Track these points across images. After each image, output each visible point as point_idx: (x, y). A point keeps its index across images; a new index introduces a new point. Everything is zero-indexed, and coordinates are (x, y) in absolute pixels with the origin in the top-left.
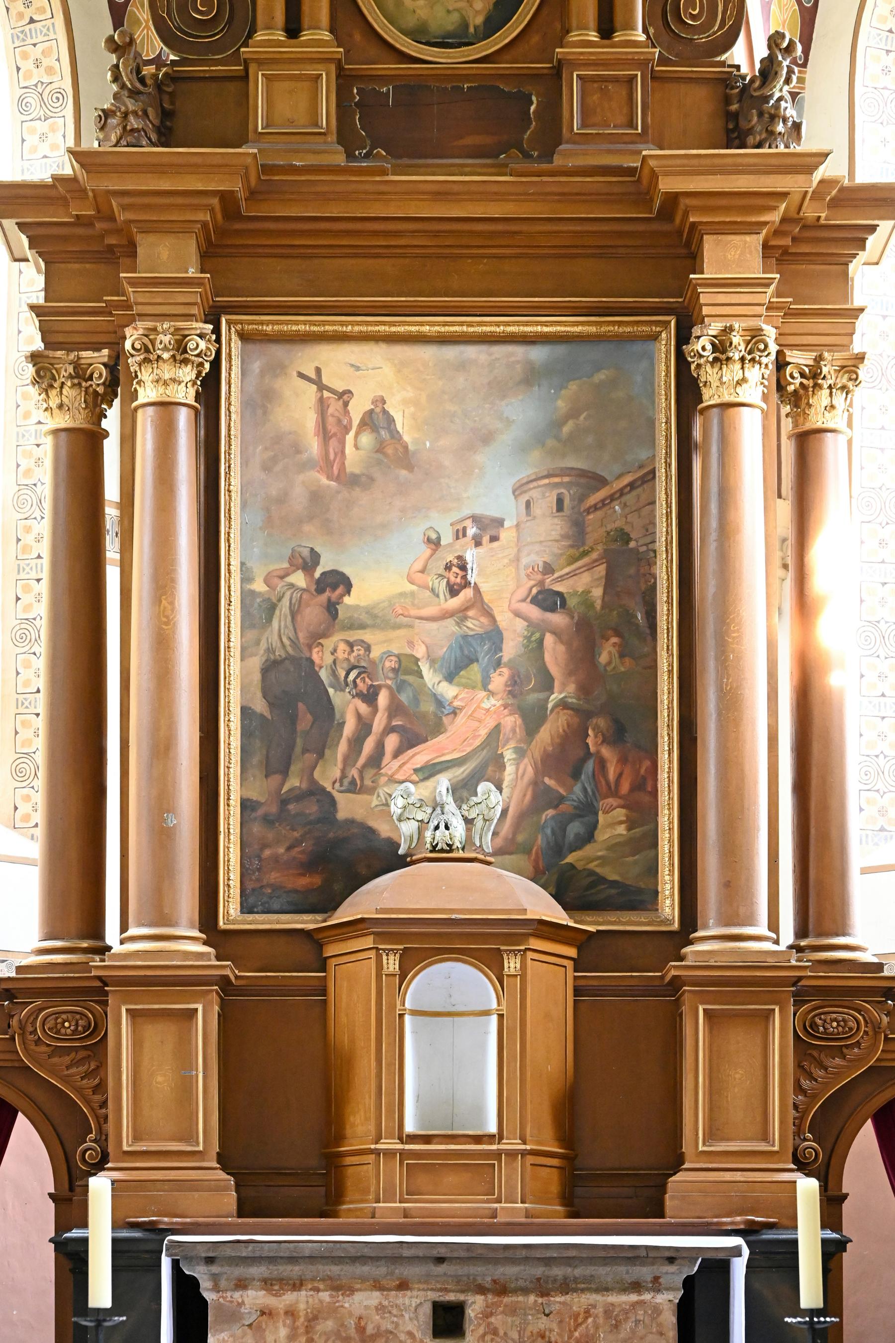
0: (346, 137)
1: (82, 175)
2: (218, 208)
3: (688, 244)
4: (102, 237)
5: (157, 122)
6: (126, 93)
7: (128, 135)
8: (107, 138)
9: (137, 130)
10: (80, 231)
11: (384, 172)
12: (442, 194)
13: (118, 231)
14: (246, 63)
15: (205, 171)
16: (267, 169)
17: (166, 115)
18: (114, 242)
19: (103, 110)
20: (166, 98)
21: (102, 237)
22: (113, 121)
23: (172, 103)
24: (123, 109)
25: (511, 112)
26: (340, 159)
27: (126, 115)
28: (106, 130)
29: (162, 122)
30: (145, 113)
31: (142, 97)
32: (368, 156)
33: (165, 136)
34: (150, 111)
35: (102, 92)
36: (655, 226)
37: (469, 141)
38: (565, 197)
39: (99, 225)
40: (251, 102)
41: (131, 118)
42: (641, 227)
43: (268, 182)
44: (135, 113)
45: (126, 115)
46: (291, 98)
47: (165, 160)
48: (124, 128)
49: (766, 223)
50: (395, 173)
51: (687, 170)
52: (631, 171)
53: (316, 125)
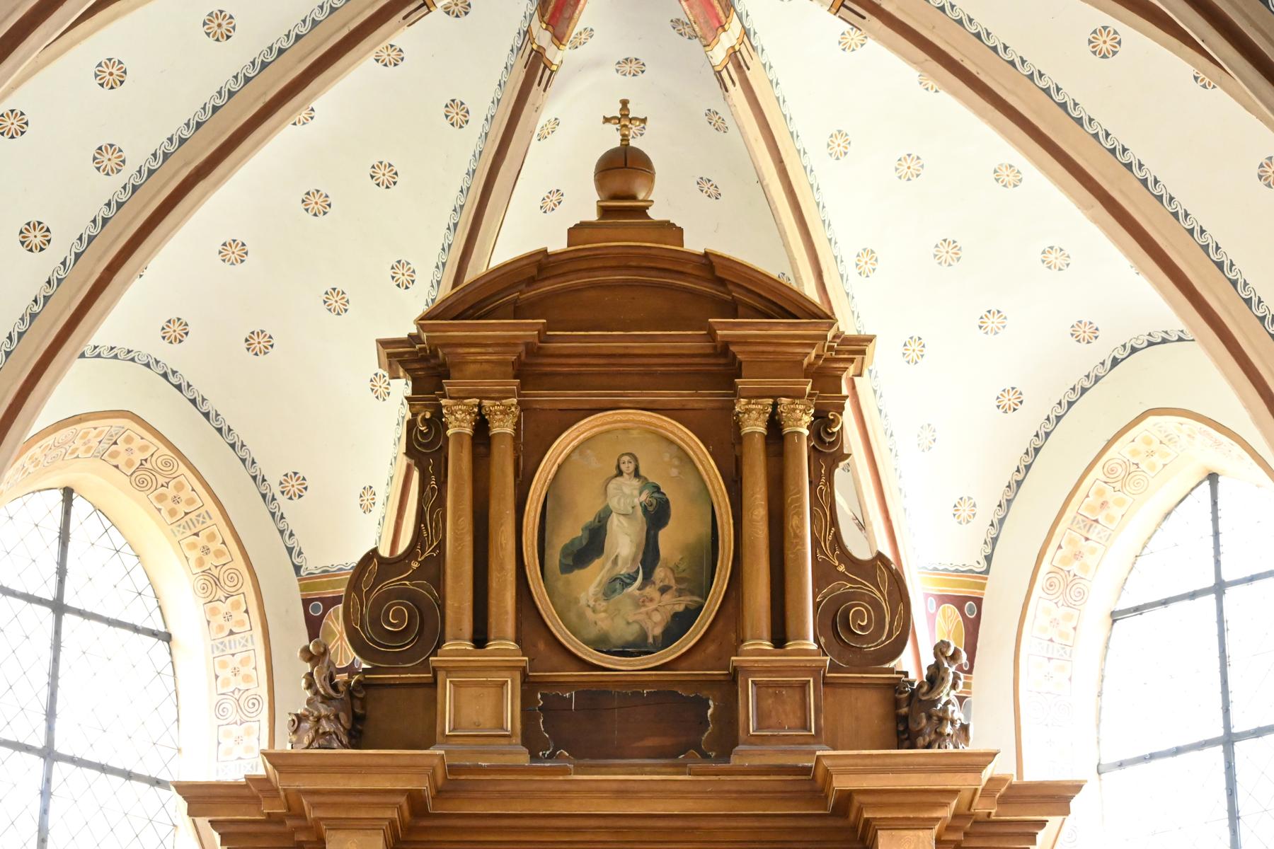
0: (530, 740)
1: (274, 775)
2: (405, 807)
3: (863, 839)
4: (292, 834)
5: (348, 726)
6: (319, 699)
7: (321, 737)
8: (300, 741)
9: (329, 733)
10: (273, 828)
11: (566, 772)
12: (622, 793)
13: (308, 829)
14: (435, 670)
15: (393, 771)
16: (453, 769)
17: (357, 719)
18: (304, 839)
19: (297, 715)
20: (357, 704)
21: (292, 834)
22: (306, 725)
23: (363, 708)
24: (316, 713)
25: (690, 714)
26: (524, 759)
27: (318, 719)
28: (300, 733)
29: (353, 725)
30: (337, 717)
31: (334, 703)
32: (551, 757)
33: (356, 738)
34: (342, 716)
35: (296, 698)
36: (830, 823)
37: (650, 742)
38: (743, 795)
39: (289, 823)
40: (439, 707)
41: (324, 722)
42: (817, 823)
43: (455, 781)
44: (327, 717)
45: (318, 719)
46: (478, 702)
47: (357, 761)
48: (317, 731)
49: (938, 819)
50: (576, 773)
51: (860, 768)
52: (806, 771)
53: (502, 728)
